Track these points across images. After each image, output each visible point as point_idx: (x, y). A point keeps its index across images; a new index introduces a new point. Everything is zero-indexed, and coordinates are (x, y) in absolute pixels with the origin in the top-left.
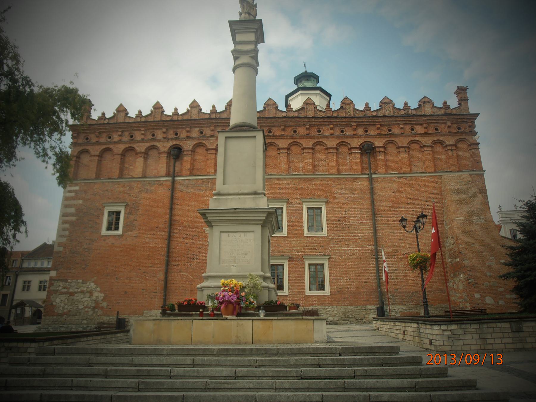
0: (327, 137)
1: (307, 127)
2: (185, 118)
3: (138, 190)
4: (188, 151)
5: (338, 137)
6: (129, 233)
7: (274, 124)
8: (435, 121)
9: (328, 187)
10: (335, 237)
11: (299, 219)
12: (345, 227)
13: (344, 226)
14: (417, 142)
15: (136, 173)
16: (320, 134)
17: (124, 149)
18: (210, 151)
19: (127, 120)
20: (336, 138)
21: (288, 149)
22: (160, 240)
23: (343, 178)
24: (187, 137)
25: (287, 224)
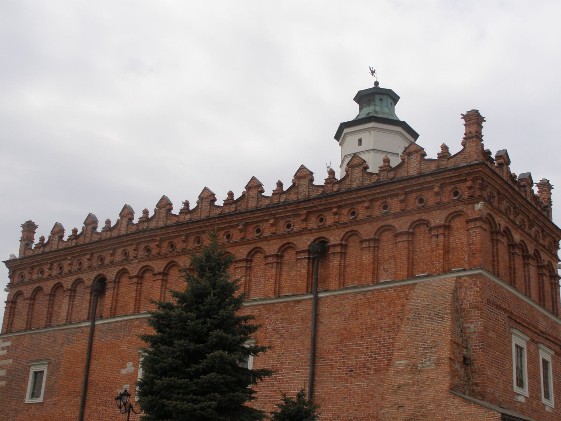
0: (267, 239)
6: (50, 400)
8: (418, 187)
10: (261, 396)
12: (275, 381)
13: (273, 379)
14: (389, 228)
17: (54, 287)
20: (279, 239)
23: (281, 302)
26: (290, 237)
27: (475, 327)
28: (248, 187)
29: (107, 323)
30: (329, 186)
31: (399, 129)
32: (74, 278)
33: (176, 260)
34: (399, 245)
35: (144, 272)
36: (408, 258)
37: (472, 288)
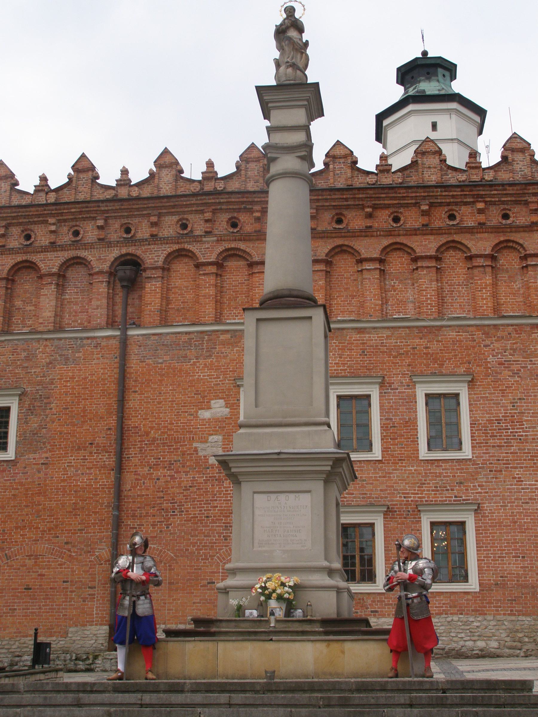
0: (470, 230)
1: (425, 208)
2: (146, 192)
3: (48, 360)
4: (156, 268)
5: (497, 230)
6: (31, 456)
7: (349, 203)
9: (474, 347)
10: (489, 460)
11: (407, 422)
12: (511, 439)
13: (510, 436)
15: (41, 321)
16: (455, 223)
18: (204, 268)
19: (16, 201)
20: (491, 232)
21: (381, 261)
22: (100, 471)
23: (508, 325)
24: (152, 236)
25: (381, 433)
26: (511, 232)
29: (154, 334)
35: (225, 259)
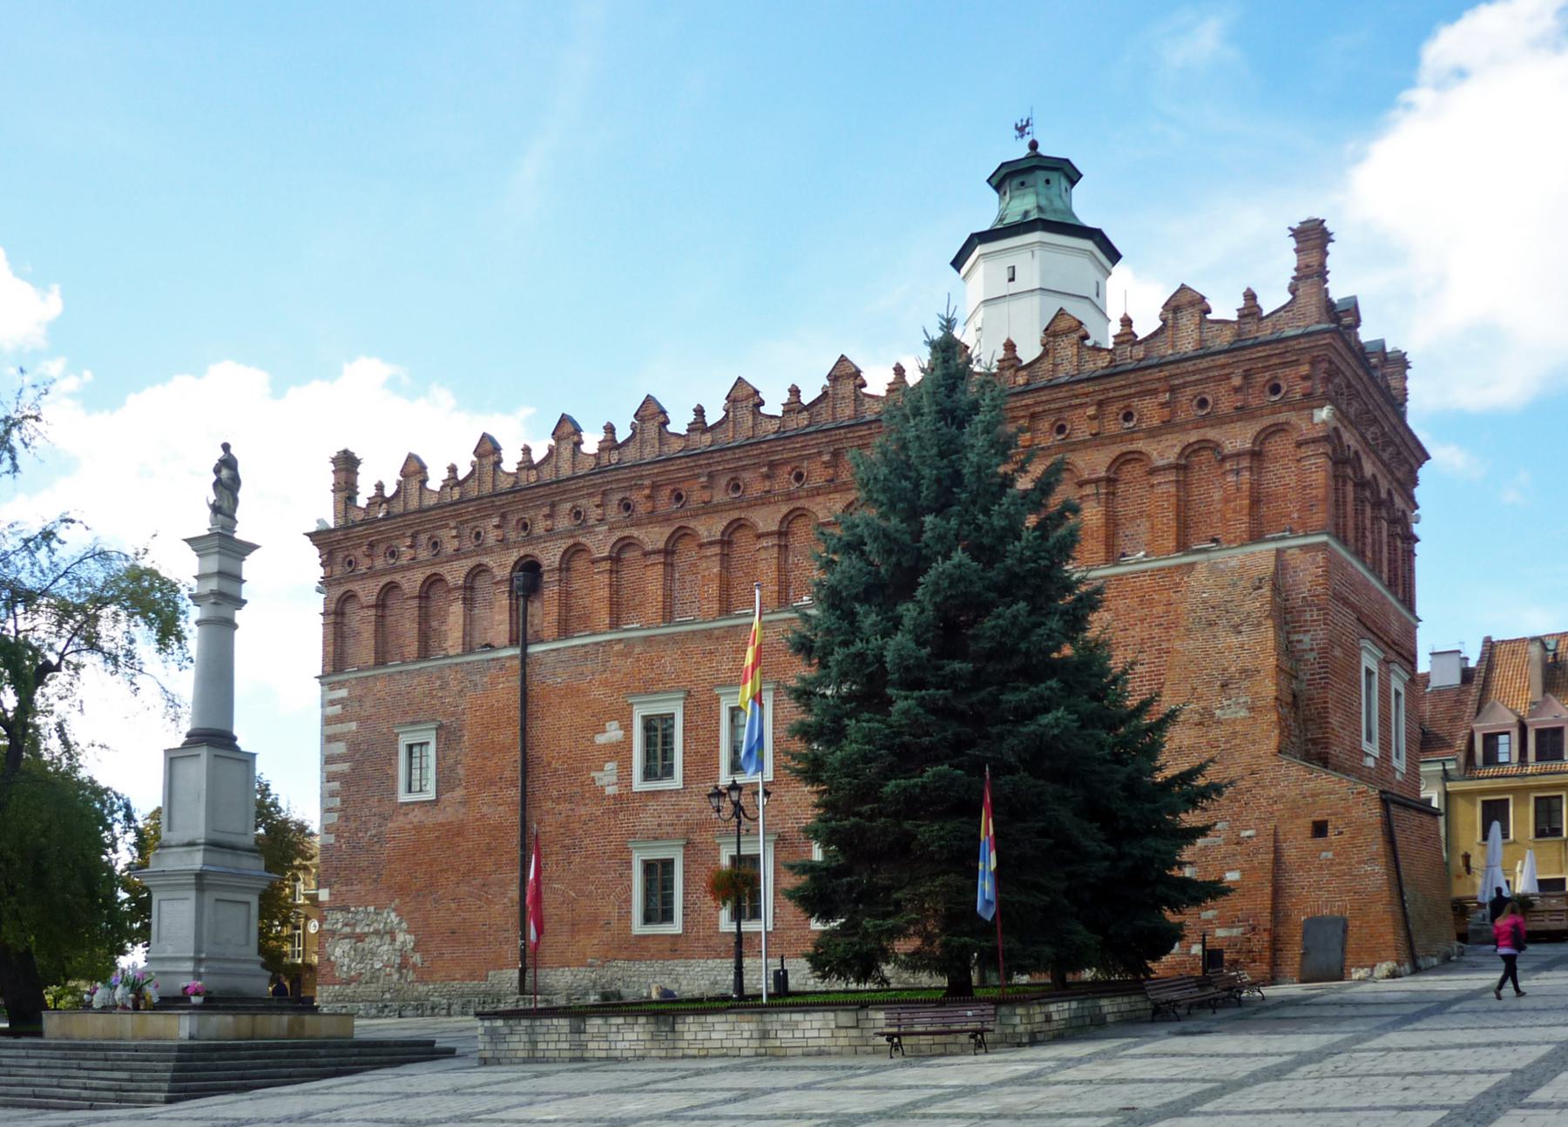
7: (744, 463)
14: (1137, 457)
17: (424, 582)
27: (1312, 640)
28: (834, 377)
29: (553, 650)
30: (1007, 373)
31: (1088, 245)
32: (468, 563)
33: (692, 525)
34: (1158, 490)
35: (621, 550)
36: (1178, 516)
37: (1307, 569)
